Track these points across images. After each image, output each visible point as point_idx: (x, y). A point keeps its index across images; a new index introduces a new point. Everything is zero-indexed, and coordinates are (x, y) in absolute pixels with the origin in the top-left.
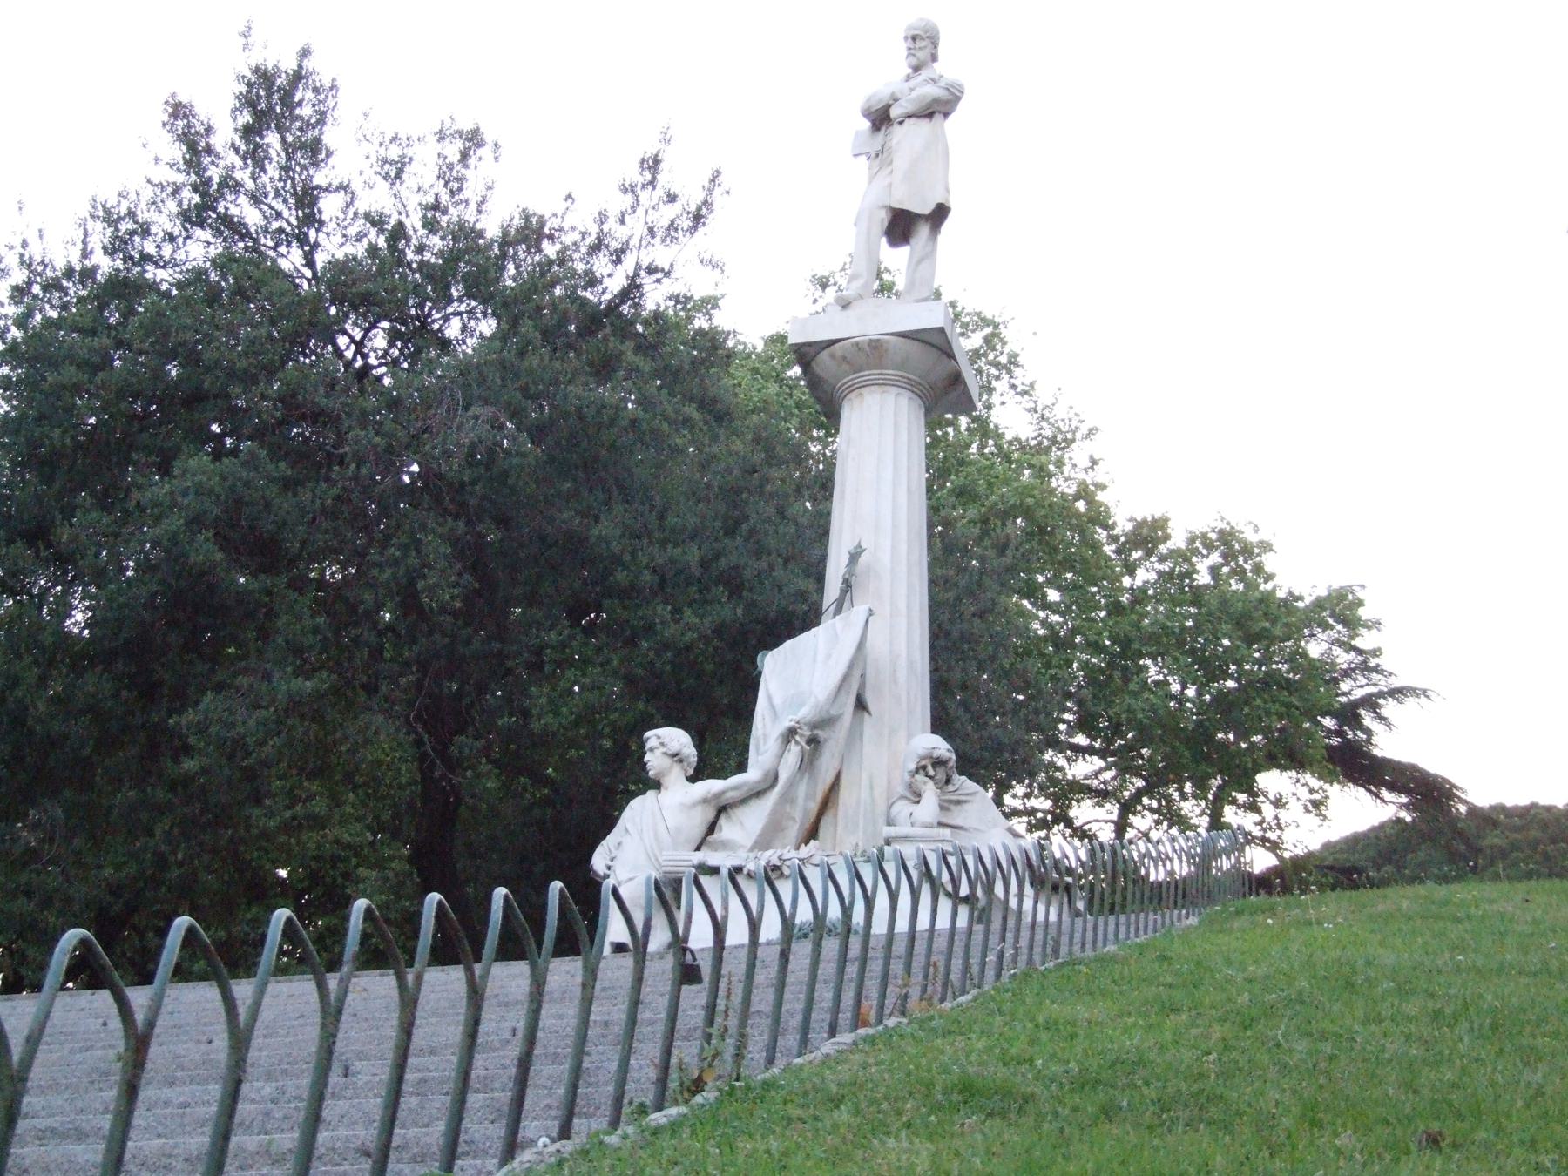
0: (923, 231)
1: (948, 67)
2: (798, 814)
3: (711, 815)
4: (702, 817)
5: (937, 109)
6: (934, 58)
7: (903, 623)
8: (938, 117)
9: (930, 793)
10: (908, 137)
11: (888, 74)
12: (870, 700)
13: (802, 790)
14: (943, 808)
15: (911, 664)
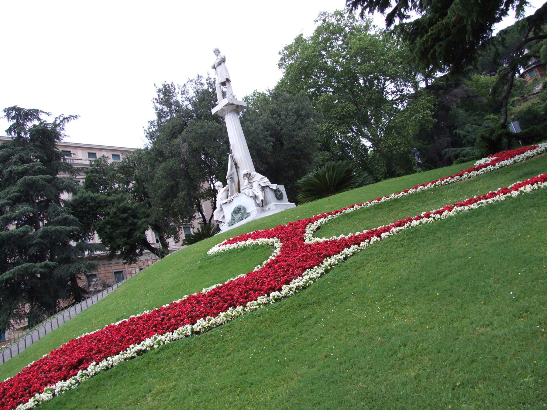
0: (227, 83)
1: (222, 55)
2: (234, 189)
3: (226, 192)
4: (225, 194)
5: (223, 60)
6: (220, 53)
7: (241, 151)
8: (222, 64)
9: (246, 179)
10: (219, 69)
11: (215, 60)
12: (239, 166)
13: (233, 185)
14: (248, 180)
15: (244, 157)
